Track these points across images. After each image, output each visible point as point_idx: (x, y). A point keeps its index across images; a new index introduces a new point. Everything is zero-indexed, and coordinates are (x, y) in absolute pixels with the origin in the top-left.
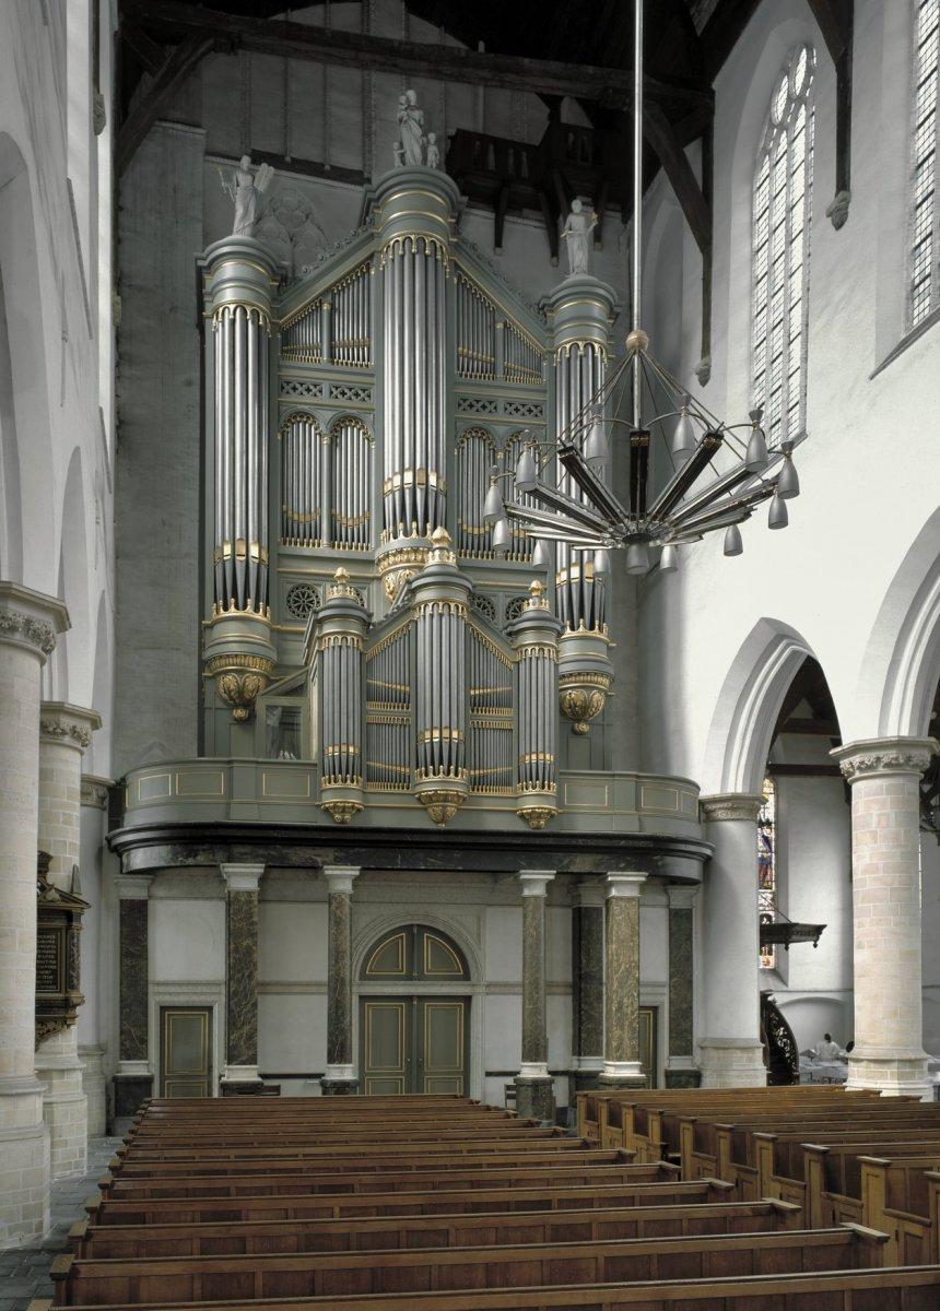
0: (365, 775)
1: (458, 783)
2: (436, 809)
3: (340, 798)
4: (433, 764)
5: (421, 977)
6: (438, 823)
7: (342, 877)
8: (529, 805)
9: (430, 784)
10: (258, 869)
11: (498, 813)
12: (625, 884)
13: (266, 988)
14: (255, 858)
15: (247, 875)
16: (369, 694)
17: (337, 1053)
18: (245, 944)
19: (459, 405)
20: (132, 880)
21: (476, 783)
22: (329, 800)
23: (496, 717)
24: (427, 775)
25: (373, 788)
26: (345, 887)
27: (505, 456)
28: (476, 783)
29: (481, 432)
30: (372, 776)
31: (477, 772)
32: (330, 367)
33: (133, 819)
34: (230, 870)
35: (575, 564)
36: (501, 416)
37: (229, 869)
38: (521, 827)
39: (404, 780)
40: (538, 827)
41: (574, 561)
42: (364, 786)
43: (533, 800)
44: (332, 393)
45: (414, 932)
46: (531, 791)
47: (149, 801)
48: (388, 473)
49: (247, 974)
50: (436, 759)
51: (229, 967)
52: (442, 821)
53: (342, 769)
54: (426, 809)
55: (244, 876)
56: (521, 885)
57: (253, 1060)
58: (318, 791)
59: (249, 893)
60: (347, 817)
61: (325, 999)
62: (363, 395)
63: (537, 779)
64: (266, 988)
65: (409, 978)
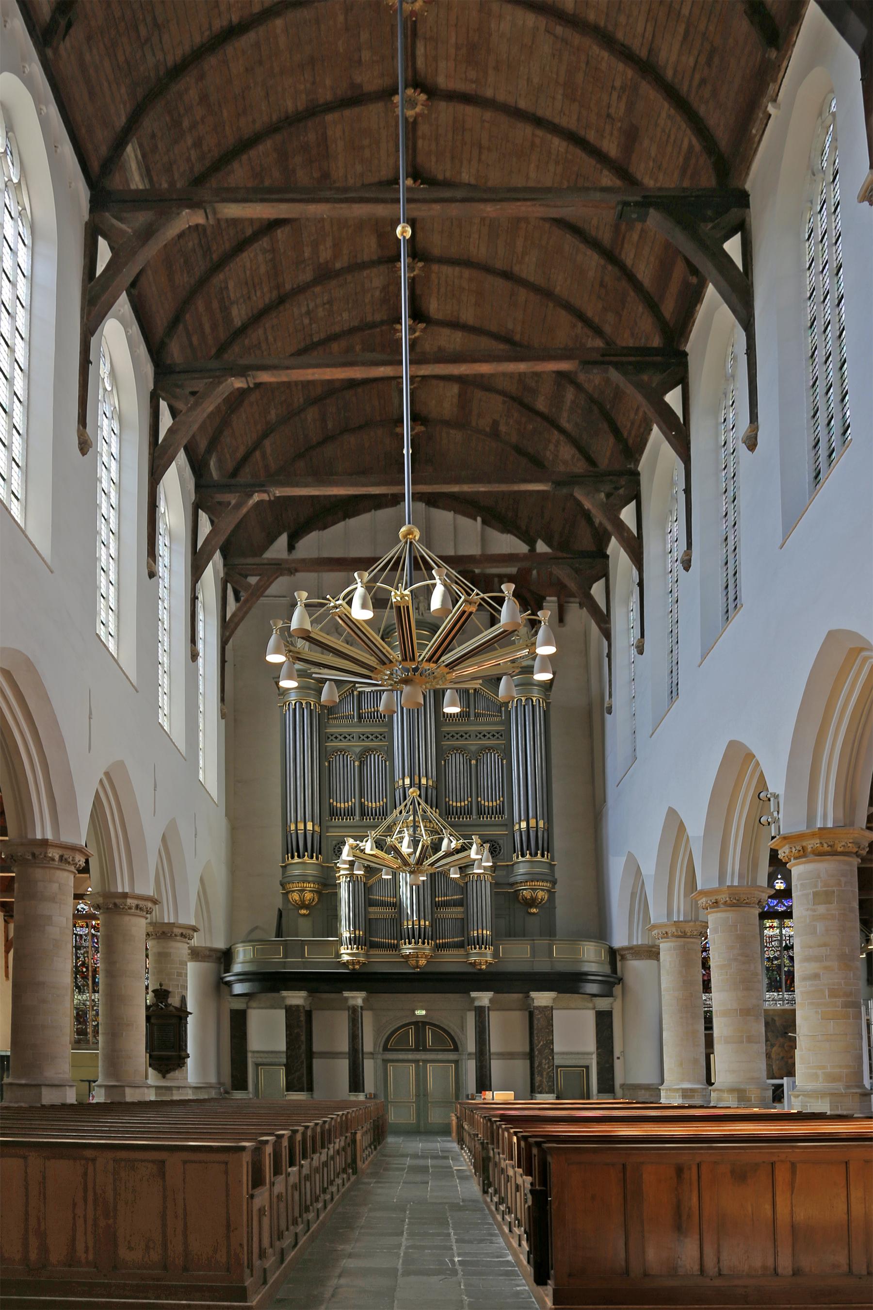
0: (368, 944)
4: (414, 938)
6: (414, 968)
9: (407, 949)
10: (303, 994)
14: (300, 989)
15: (297, 997)
16: (370, 903)
17: (356, 1084)
18: (296, 1031)
19: (445, 736)
20: (235, 999)
22: (346, 958)
24: (405, 944)
27: (477, 762)
28: (439, 947)
29: (461, 750)
30: (373, 945)
31: (441, 941)
32: (359, 724)
34: (285, 995)
35: (523, 821)
37: (285, 993)
38: (470, 969)
40: (481, 969)
41: (522, 818)
42: (368, 951)
44: (360, 737)
46: (477, 951)
48: (397, 779)
49: (297, 1046)
50: (413, 936)
52: (417, 967)
54: (407, 961)
58: (339, 955)
59: (298, 1006)
60: (357, 967)
62: (380, 737)
63: (483, 944)
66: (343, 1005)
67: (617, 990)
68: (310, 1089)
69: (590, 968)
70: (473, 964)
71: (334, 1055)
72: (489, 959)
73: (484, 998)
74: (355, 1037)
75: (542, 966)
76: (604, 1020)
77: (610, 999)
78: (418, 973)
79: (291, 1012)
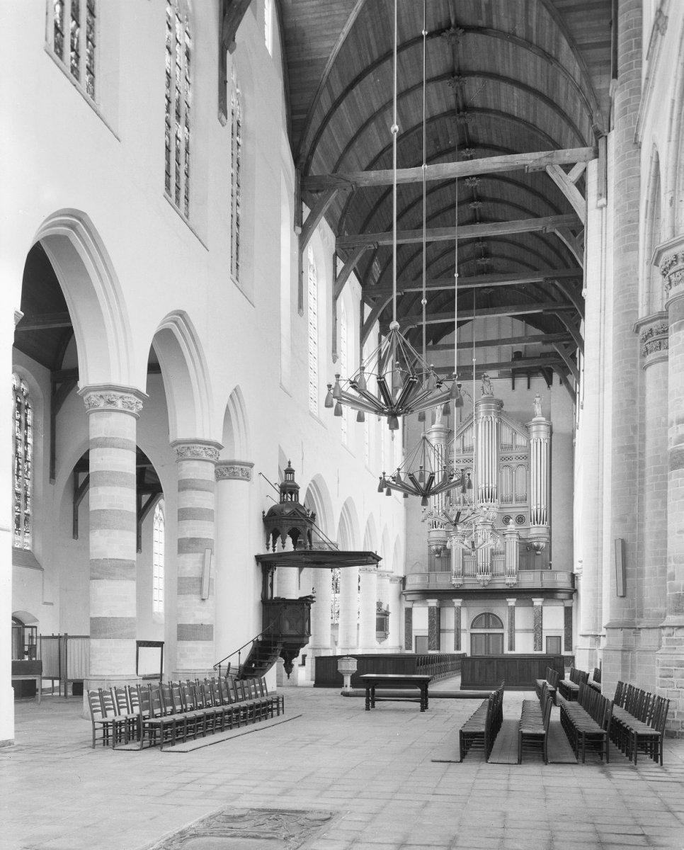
1: (488, 577)
2: (482, 583)
3: (456, 582)
5: (489, 628)
7: (458, 602)
8: (508, 581)
10: (436, 600)
11: (499, 585)
12: (538, 602)
13: (445, 631)
17: (458, 647)
21: (493, 575)
22: (454, 582)
23: (498, 558)
25: (466, 578)
26: (460, 605)
33: (408, 588)
36: (514, 461)
37: (429, 601)
38: (507, 587)
39: (475, 576)
43: (510, 581)
45: (487, 615)
47: (414, 583)
51: (429, 626)
53: (457, 575)
55: (433, 603)
56: (508, 602)
57: (439, 649)
58: (451, 581)
61: (453, 634)
64: (445, 631)
65: (485, 628)
66: (452, 605)
67: (574, 596)
68: (439, 649)
69: (560, 586)
70: (508, 584)
71: (449, 631)
72: (515, 582)
73: (512, 602)
74: (458, 622)
75: (538, 585)
76: (568, 613)
77: (571, 601)
78: (484, 590)
79: (431, 609)
